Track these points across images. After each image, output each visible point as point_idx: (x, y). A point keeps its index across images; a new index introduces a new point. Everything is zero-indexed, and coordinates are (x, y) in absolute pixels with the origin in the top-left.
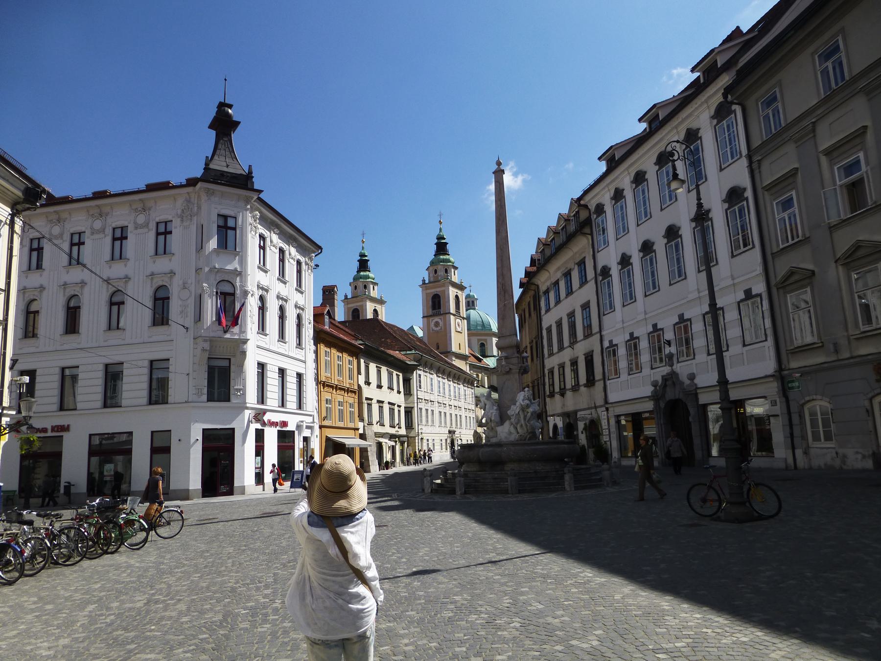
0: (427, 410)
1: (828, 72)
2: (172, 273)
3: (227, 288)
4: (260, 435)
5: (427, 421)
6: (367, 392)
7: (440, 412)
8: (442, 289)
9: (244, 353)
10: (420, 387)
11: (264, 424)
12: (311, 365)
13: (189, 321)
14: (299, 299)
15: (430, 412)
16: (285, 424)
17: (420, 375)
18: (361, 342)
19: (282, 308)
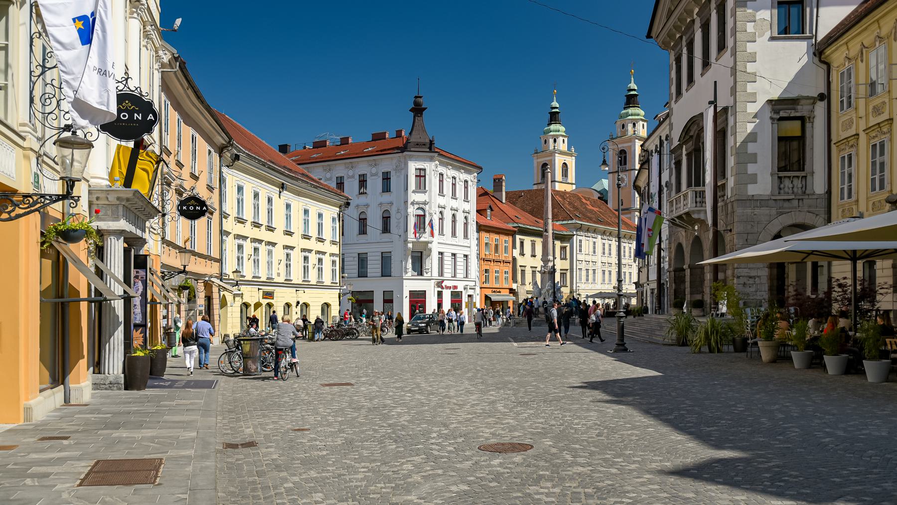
0: (587, 270)
1: (701, 130)
2: (392, 203)
3: (421, 212)
4: (440, 294)
5: (587, 280)
6: (520, 261)
7: (604, 272)
8: (629, 144)
9: (430, 250)
10: (580, 251)
11: (442, 288)
12: (474, 248)
13: (401, 232)
14: (467, 206)
15: (591, 272)
16: (455, 287)
17: (581, 241)
18: (516, 225)
19: (454, 215)
